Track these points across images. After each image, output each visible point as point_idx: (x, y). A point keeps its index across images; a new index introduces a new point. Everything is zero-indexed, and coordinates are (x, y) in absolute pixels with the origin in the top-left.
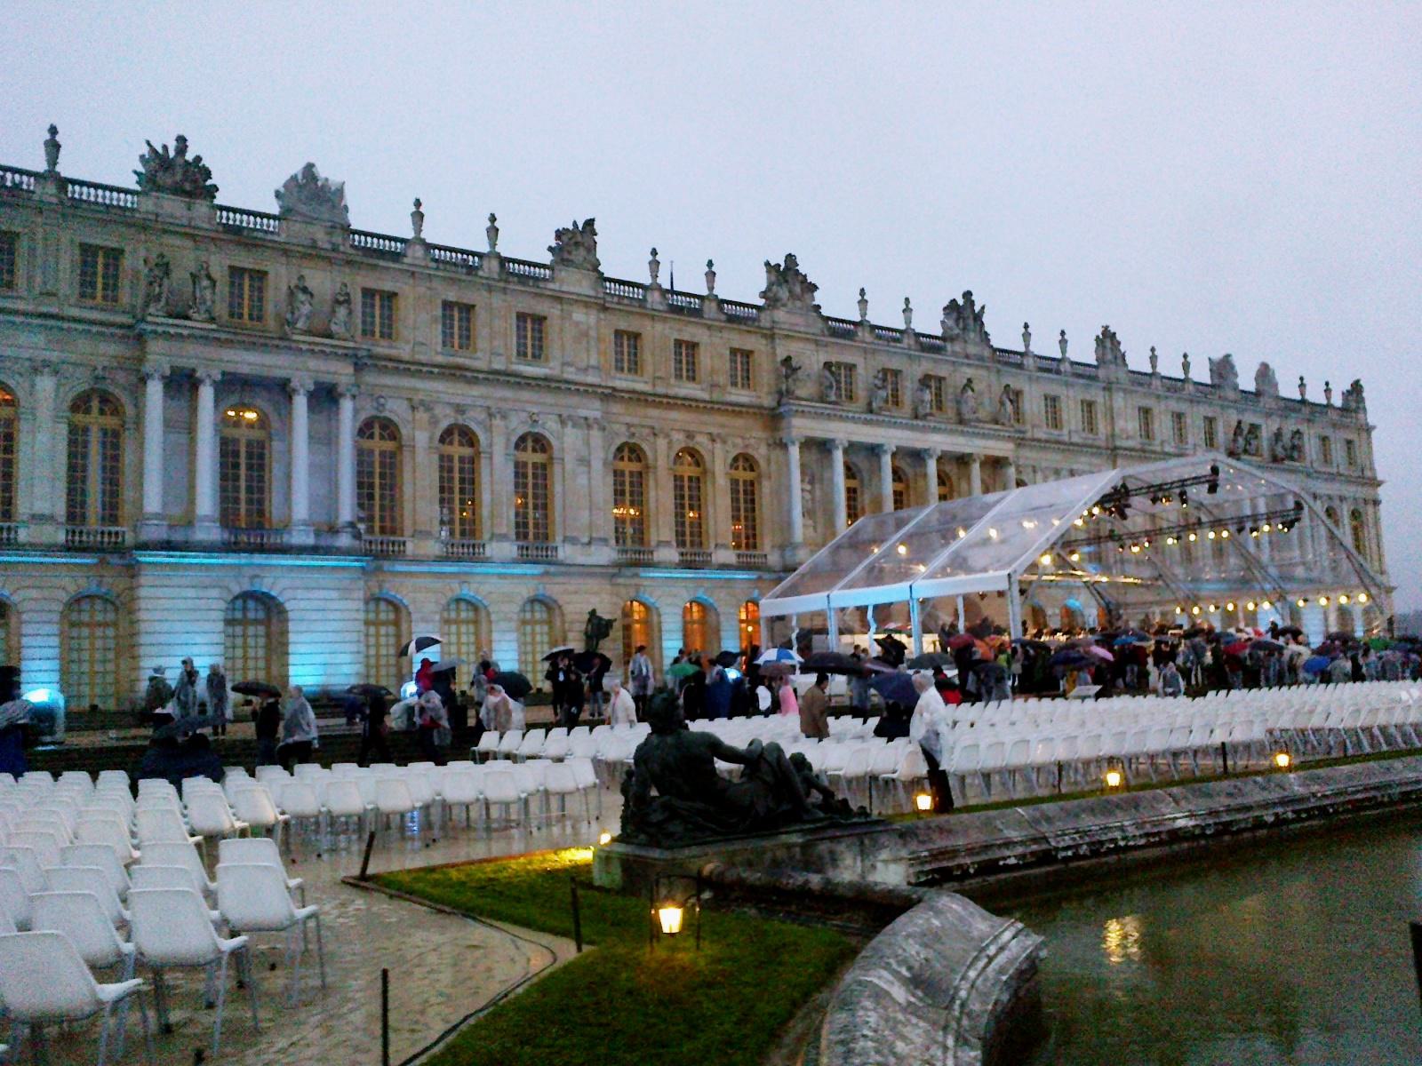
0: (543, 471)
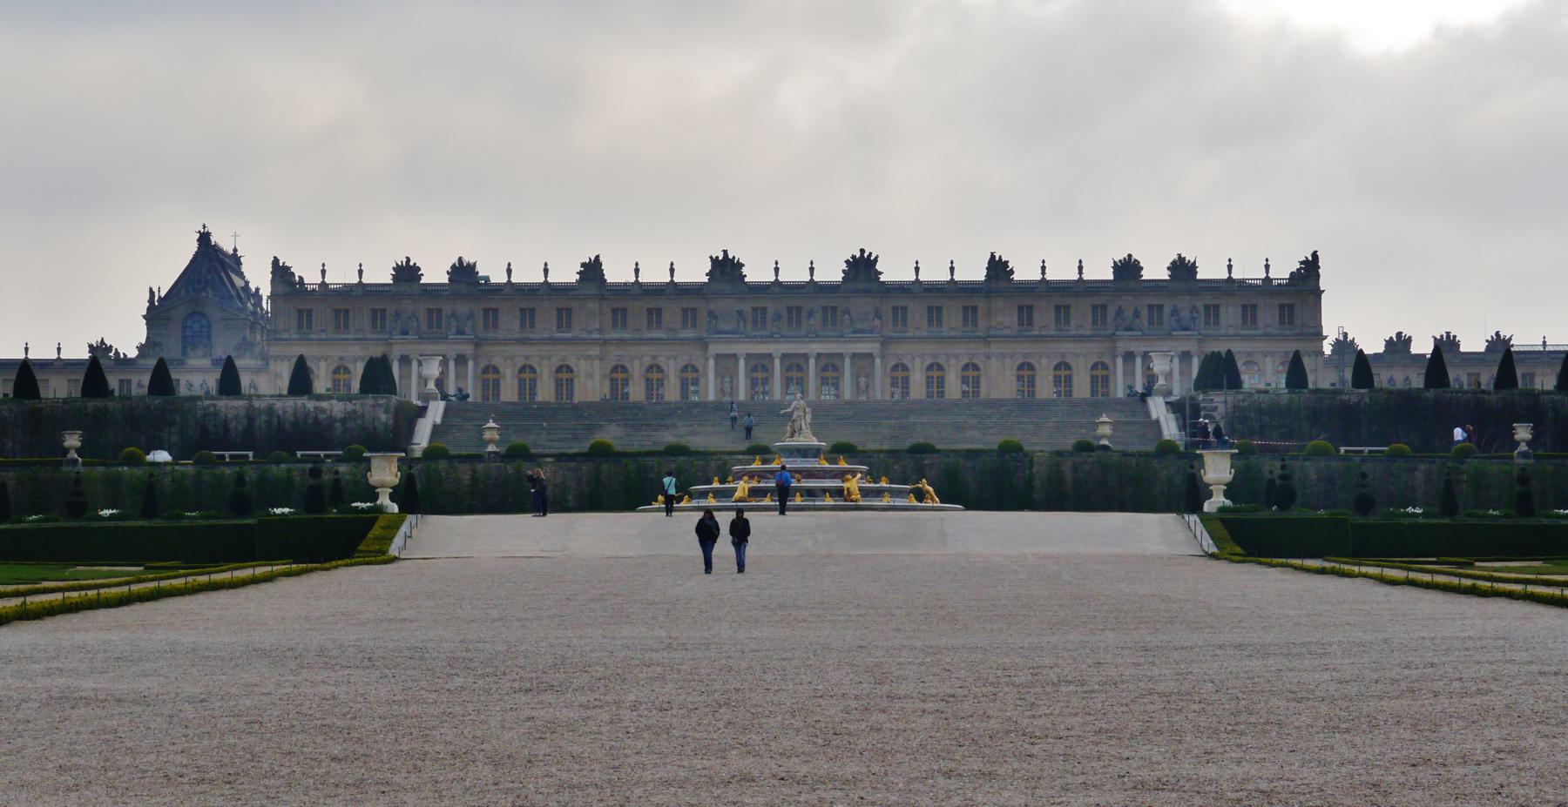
0: (571, 382)
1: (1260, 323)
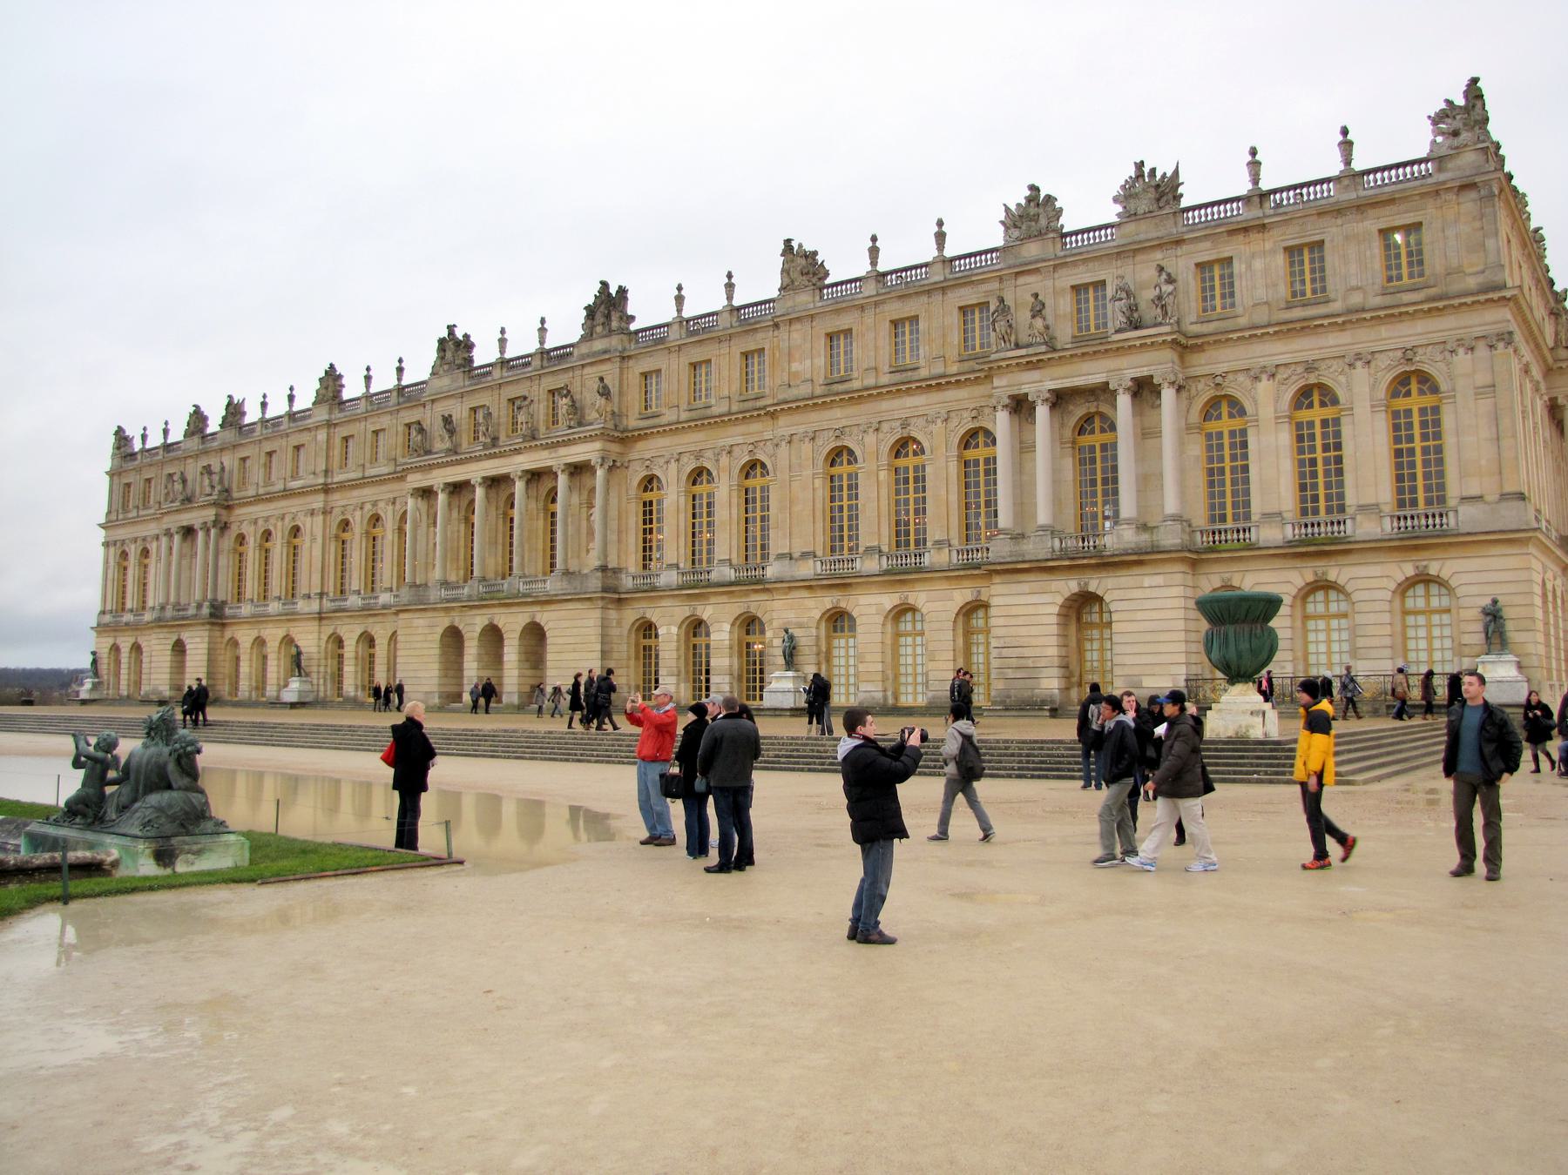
1: (1334, 284)
